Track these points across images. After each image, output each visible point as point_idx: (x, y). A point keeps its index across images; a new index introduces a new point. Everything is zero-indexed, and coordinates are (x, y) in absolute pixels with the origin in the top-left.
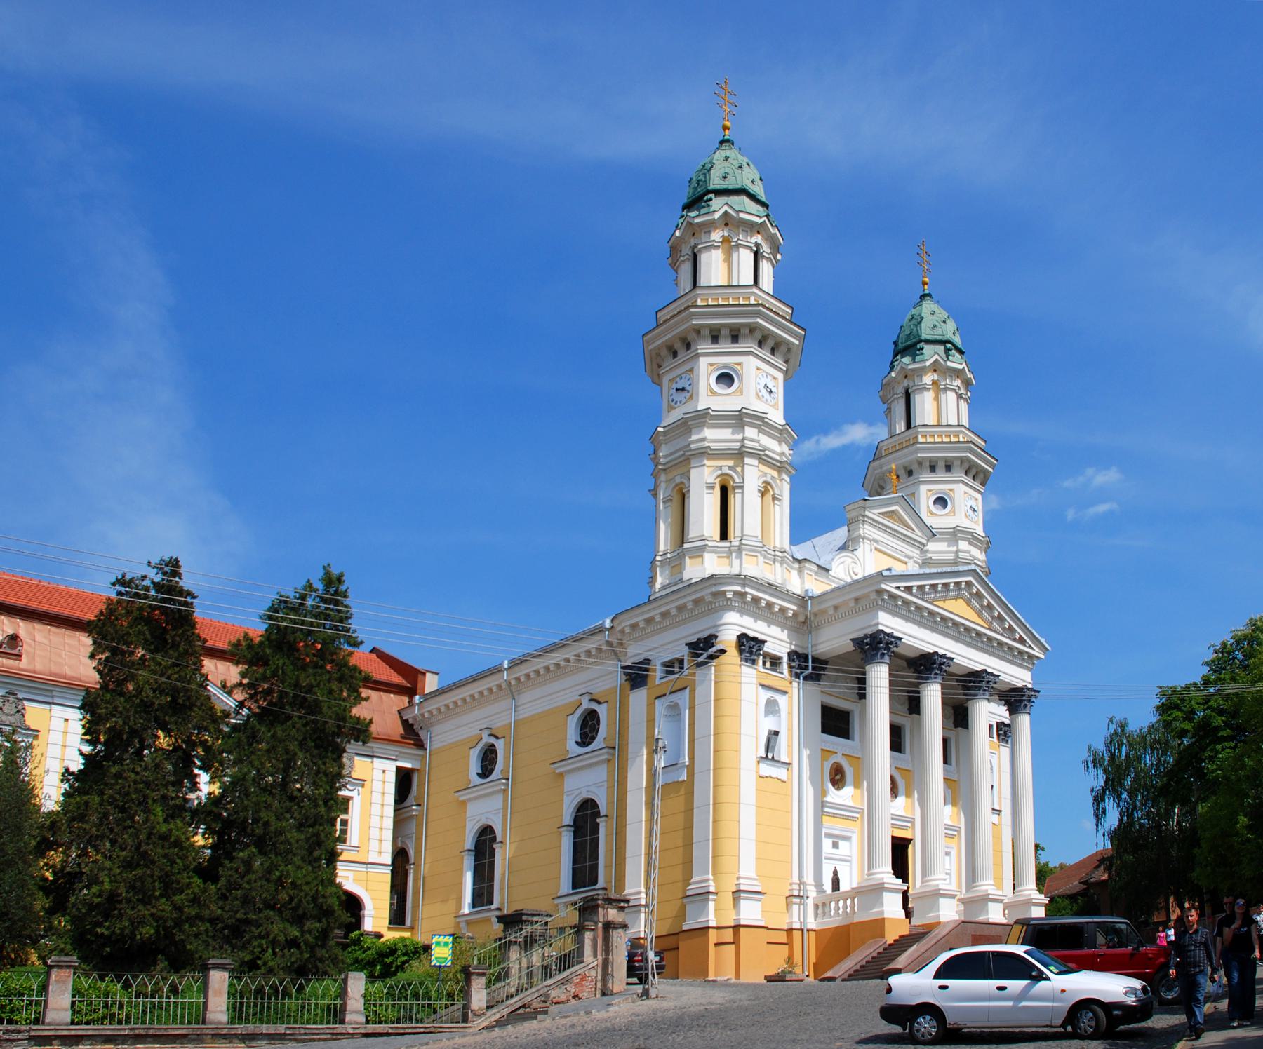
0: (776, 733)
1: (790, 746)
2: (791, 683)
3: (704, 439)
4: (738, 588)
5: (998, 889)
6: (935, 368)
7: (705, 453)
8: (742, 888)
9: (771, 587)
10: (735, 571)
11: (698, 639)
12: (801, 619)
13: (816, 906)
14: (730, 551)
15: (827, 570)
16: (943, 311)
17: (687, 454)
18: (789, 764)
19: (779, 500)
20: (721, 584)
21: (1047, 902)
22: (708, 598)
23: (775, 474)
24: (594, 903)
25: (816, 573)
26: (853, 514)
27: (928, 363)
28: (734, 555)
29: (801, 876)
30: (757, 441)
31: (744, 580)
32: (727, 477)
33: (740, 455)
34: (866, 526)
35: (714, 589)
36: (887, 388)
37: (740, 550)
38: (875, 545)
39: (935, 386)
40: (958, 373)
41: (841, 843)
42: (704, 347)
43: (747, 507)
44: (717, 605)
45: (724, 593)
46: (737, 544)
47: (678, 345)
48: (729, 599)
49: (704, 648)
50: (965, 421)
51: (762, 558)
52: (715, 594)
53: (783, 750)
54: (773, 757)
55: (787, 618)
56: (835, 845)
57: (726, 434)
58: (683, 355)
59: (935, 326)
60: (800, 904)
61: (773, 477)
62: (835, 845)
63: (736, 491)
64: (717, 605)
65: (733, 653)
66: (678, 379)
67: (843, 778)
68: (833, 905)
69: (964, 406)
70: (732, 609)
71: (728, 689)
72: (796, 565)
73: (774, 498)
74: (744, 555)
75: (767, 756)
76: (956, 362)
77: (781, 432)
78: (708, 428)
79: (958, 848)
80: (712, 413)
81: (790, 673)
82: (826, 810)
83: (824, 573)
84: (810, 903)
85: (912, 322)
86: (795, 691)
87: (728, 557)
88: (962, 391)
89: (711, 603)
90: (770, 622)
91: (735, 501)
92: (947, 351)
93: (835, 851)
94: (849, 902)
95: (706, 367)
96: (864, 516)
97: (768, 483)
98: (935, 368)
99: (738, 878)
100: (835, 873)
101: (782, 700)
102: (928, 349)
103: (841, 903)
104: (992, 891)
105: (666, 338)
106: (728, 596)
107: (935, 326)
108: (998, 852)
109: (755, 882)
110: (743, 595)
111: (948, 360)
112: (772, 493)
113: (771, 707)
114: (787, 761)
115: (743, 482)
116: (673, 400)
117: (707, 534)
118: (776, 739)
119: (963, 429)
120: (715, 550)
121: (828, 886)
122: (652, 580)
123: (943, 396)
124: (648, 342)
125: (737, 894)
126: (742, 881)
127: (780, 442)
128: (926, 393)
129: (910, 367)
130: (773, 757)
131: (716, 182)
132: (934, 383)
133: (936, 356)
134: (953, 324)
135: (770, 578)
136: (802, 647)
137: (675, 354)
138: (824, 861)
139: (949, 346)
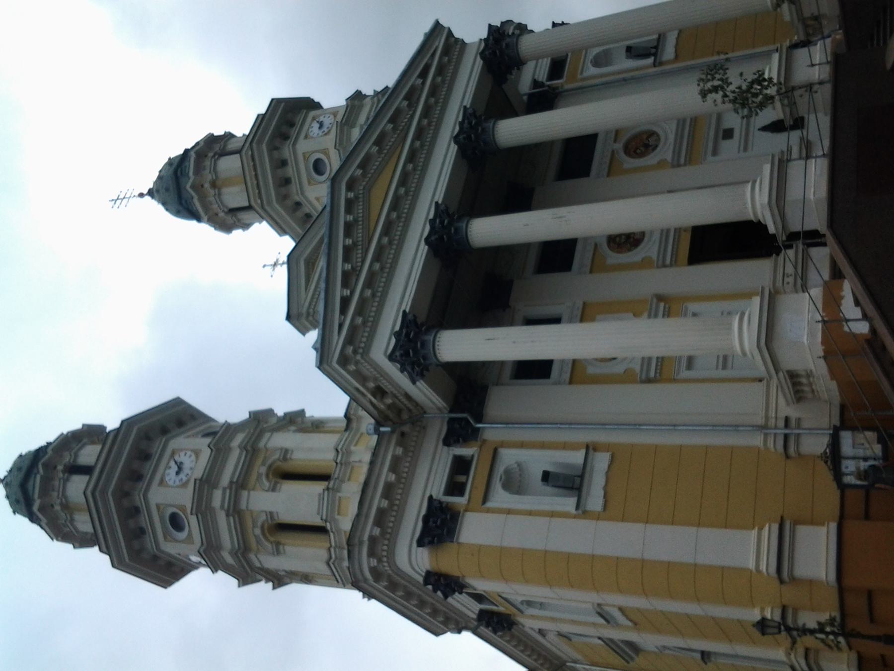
1: (565, 446)
2: (484, 441)
18: (587, 447)
30: (224, 489)
39: (218, 183)
46: (328, 524)
61: (263, 464)
72: (354, 425)
73: (285, 459)
82: (652, 374)
91: (287, 517)
96: (308, 314)
97: (270, 467)
106: (376, 564)
107: (167, 190)
110: (373, 540)
114: (583, 452)
115: (266, 512)
118: (557, 476)
126: (763, 568)
133: (188, 187)
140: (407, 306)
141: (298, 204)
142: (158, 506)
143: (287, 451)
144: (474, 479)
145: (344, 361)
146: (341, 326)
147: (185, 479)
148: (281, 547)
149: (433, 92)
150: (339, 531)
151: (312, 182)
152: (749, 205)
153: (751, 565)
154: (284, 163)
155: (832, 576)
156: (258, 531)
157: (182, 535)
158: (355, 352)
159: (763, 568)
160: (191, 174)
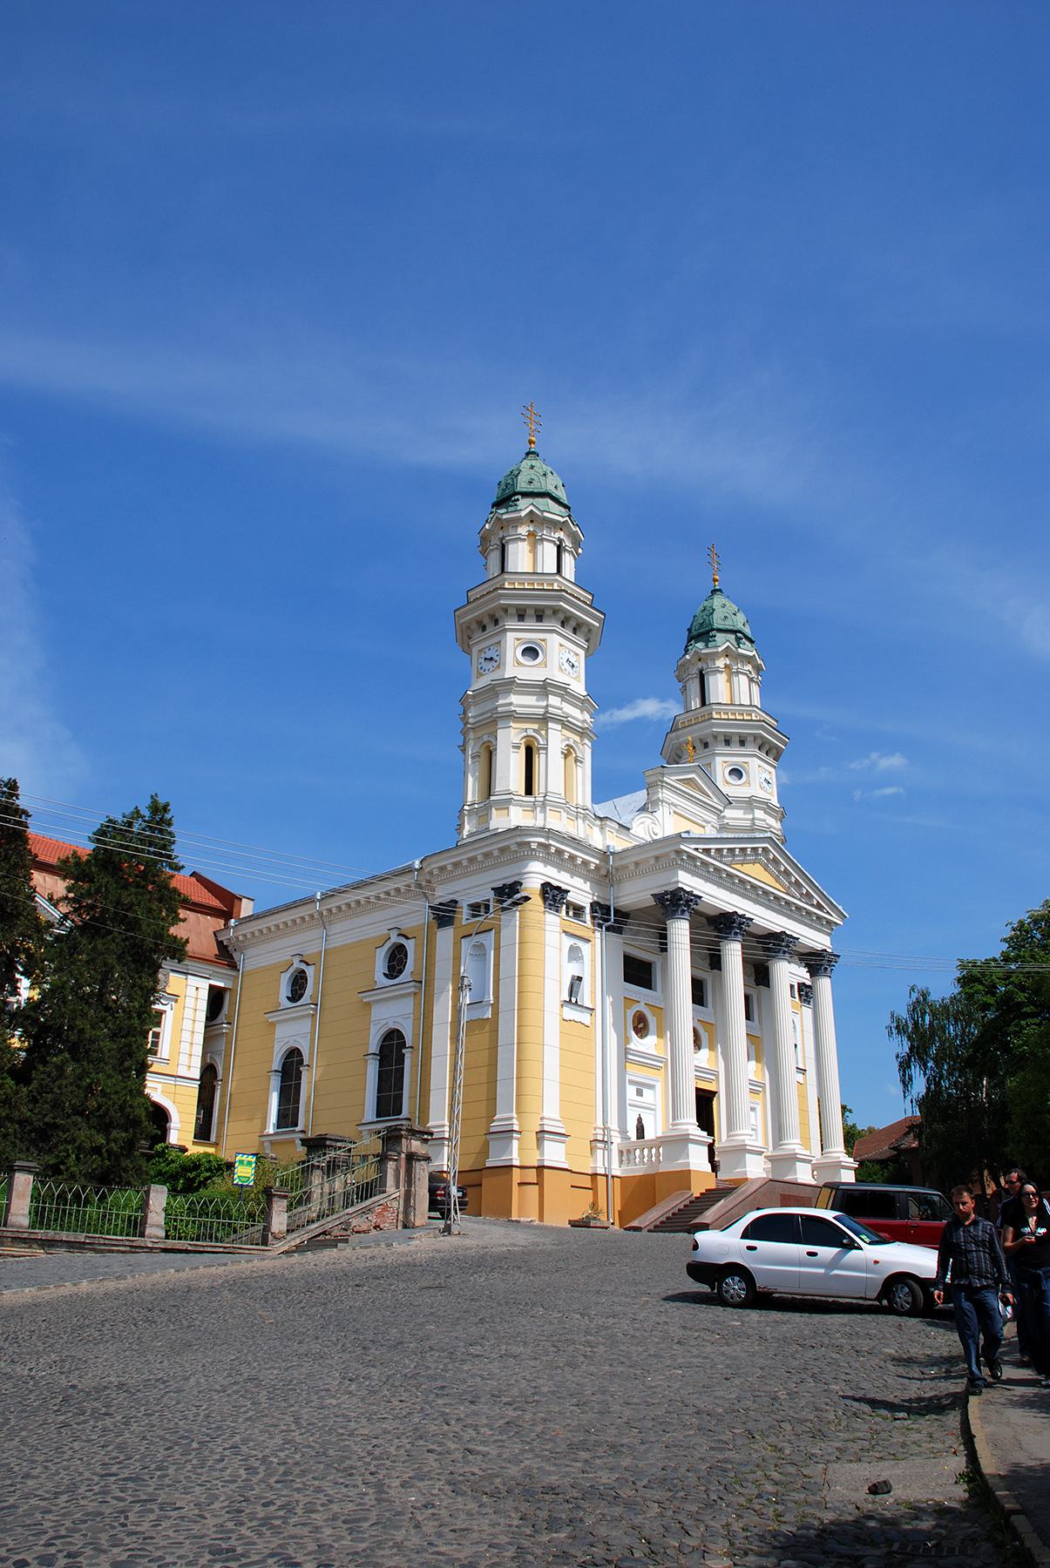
0: (580, 979)
1: (593, 992)
3: (511, 704)
4: (542, 840)
5: (806, 1149)
6: (727, 653)
7: (511, 716)
8: (546, 1128)
9: (574, 841)
10: (540, 824)
11: (504, 885)
12: (603, 872)
13: (621, 1152)
14: (535, 807)
15: (629, 829)
16: (734, 606)
17: (494, 716)
18: (593, 1009)
19: (582, 762)
20: (525, 835)
21: (857, 1166)
22: (514, 848)
23: (577, 739)
24: (397, 1133)
25: (617, 831)
26: (653, 779)
27: (720, 649)
28: (538, 809)
29: (605, 1121)
31: (549, 833)
32: (531, 739)
33: (544, 719)
34: (664, 791)
35: (519, 840)
36: (682, 669)
37: (544, 805)
38: (674, 808)
40: (749, 660)
41: (645, 1091)
42: (511, 624)
43: (551, 768)
44: (522, 854)
45: (529, 843)
46: (542, 799)
47: (486, 621)
48: (534, 849)
49: (509, 893)
50: (757, 702)
51: (565, 814)
52: (520, 844)
53: (586, 995)
54: (576, 1002)
55: (589, 871)
56: (639, 1093)
57: (531, 700)
58: (491, 629)
59: (726, 617)
60: (604, 1149)
62: (639, 1093)
64: (522, 854)
65: (537, 900)
66: (486, 650)
67: (646, 1027)
68: (638, 1152)
69: (755, 688)
70: (537, 859)
71: (532, 934)
72: (598, 822)
73: (576, 760)
74: (548, 811)
75: (570, 1000)
76: (746, 650)
77: (583, 702)
78: (514, 694)
79: (764, 1103)
80: (519, 682)
81: (593, 924)
82: (630, 1057)
83: (625, 831)
84: (615, 1148)
85: (705, 613)
86: (598, 942)
87: (533, 811)
88: (754, 675)
89: (516, 851)
90: (573, 874)
91: (539, 761)
92: (738, 639)
93: (639, 1098)
94: (654, 1151)
95: (513, 640)
96: (662, 782)
97: (572, 747)
98: (727, 653)
99: (542, 1119)
100: (640, 1120)
101: (585, 947)
102: (720, 637)
103: (646, 1151)
104: (800, 1150)
105: (477, 613)
108: (804, 1111)
109: (560, 1124)
110: (547, 847)
111: (739, 647)
112: (574, 755)
113: (574, 954)
116: (481, 668)
117: (512, 789)
119: (755, 709)
120: (520, 804)
121: (632, 1134)
122: (460, 827)
123: (735, 679)
124: (459, 616)
125: (541, 1133)
126: (545, 1122)
127: (582, 711)
128: (719, 675)
129: (703, 652)
130: (576, 1002)
131: (523, 485)
132: (726, 666)
133: (728, 644)
134: (743, 616)
135: (574, 833)
136: (603, 898)
137: (484, 628)
138: (628, 1107)
139: (739, 635)
140: (706, 898)
141: (706, 745)
142: (543, 640)
144: (575, 926)
145: (679, 852)
146: (697, 849)
147: (563, 668)
149: (809, 913)
151: (725, 765)
152: (739, 1132)
153: (546, 1114)
154: (742, 743)
155: (546, 1164)
156: (530, 733)
157: (519, 653)
158: (682, 859)
159: (545, 1122)
160: (740, 650)
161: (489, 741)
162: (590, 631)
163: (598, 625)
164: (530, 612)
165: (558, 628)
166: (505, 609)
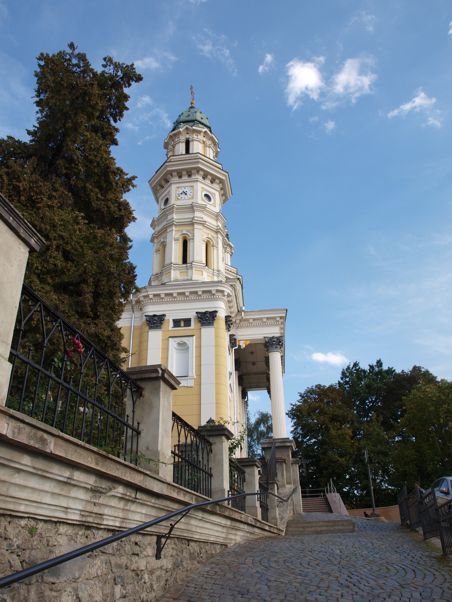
23: (215, 235)
30: (202, 218)
42: (175, 179)
58: (166, 186)
63: (191, 241)
73: (213, 246)
97: (210, 239)
112: (212, 244)
142: (192, 186)
143: (217, 247)
148: (178, 242)
150: (187, 269)
156: (185, 232)
161: (164, 241)
162: (220, 182)
163: (224, 178)
164: (184, 173)
165: (200, 178)
166: (170, 173)
